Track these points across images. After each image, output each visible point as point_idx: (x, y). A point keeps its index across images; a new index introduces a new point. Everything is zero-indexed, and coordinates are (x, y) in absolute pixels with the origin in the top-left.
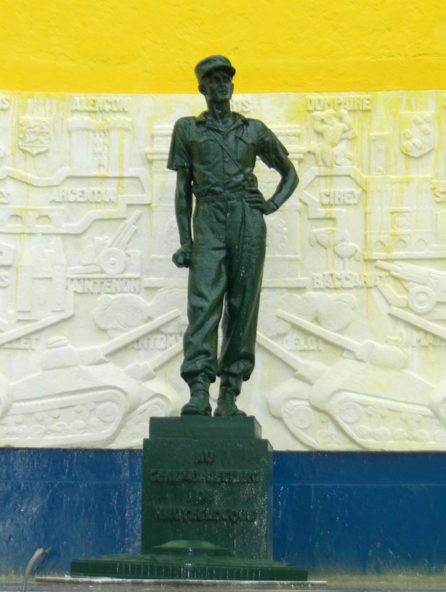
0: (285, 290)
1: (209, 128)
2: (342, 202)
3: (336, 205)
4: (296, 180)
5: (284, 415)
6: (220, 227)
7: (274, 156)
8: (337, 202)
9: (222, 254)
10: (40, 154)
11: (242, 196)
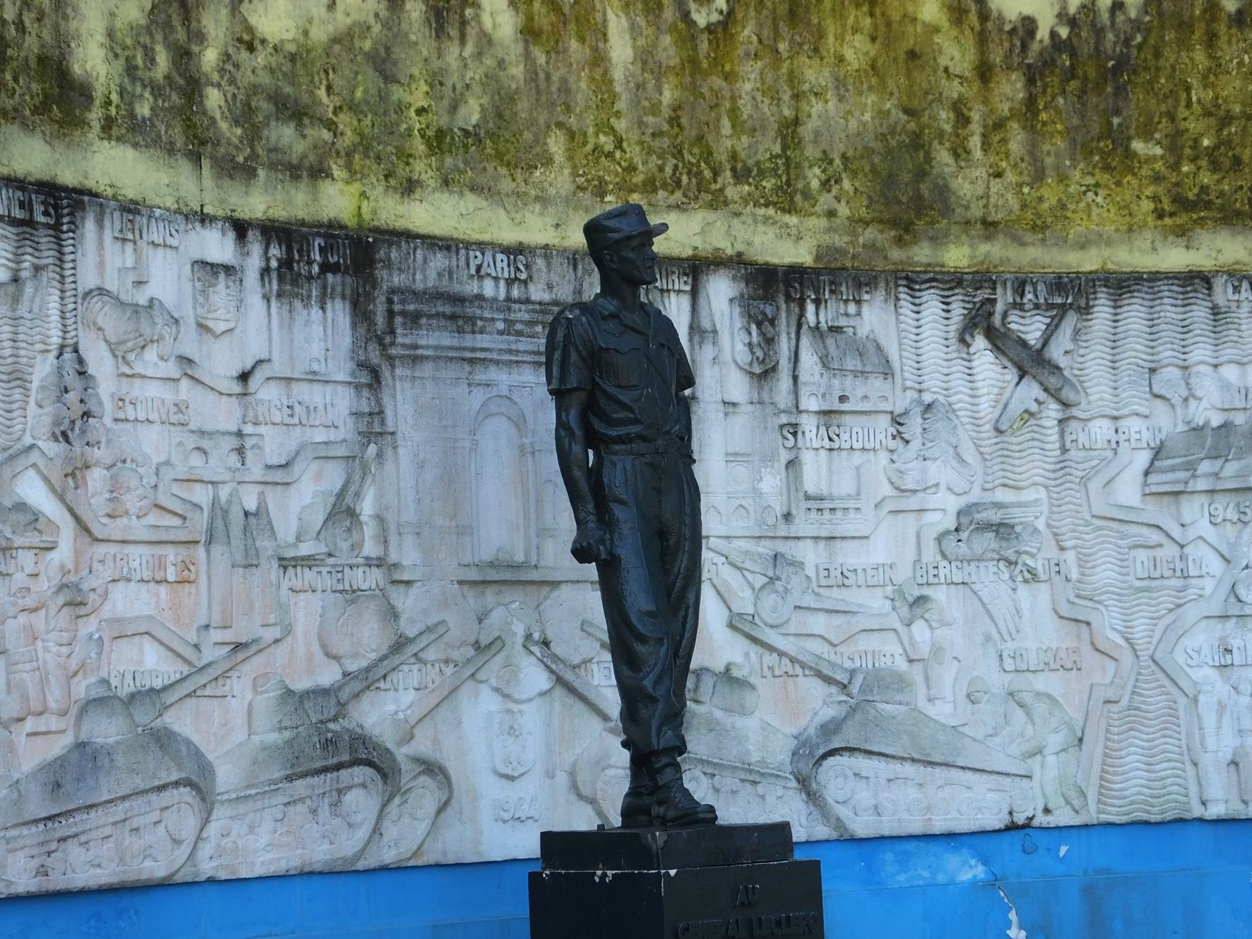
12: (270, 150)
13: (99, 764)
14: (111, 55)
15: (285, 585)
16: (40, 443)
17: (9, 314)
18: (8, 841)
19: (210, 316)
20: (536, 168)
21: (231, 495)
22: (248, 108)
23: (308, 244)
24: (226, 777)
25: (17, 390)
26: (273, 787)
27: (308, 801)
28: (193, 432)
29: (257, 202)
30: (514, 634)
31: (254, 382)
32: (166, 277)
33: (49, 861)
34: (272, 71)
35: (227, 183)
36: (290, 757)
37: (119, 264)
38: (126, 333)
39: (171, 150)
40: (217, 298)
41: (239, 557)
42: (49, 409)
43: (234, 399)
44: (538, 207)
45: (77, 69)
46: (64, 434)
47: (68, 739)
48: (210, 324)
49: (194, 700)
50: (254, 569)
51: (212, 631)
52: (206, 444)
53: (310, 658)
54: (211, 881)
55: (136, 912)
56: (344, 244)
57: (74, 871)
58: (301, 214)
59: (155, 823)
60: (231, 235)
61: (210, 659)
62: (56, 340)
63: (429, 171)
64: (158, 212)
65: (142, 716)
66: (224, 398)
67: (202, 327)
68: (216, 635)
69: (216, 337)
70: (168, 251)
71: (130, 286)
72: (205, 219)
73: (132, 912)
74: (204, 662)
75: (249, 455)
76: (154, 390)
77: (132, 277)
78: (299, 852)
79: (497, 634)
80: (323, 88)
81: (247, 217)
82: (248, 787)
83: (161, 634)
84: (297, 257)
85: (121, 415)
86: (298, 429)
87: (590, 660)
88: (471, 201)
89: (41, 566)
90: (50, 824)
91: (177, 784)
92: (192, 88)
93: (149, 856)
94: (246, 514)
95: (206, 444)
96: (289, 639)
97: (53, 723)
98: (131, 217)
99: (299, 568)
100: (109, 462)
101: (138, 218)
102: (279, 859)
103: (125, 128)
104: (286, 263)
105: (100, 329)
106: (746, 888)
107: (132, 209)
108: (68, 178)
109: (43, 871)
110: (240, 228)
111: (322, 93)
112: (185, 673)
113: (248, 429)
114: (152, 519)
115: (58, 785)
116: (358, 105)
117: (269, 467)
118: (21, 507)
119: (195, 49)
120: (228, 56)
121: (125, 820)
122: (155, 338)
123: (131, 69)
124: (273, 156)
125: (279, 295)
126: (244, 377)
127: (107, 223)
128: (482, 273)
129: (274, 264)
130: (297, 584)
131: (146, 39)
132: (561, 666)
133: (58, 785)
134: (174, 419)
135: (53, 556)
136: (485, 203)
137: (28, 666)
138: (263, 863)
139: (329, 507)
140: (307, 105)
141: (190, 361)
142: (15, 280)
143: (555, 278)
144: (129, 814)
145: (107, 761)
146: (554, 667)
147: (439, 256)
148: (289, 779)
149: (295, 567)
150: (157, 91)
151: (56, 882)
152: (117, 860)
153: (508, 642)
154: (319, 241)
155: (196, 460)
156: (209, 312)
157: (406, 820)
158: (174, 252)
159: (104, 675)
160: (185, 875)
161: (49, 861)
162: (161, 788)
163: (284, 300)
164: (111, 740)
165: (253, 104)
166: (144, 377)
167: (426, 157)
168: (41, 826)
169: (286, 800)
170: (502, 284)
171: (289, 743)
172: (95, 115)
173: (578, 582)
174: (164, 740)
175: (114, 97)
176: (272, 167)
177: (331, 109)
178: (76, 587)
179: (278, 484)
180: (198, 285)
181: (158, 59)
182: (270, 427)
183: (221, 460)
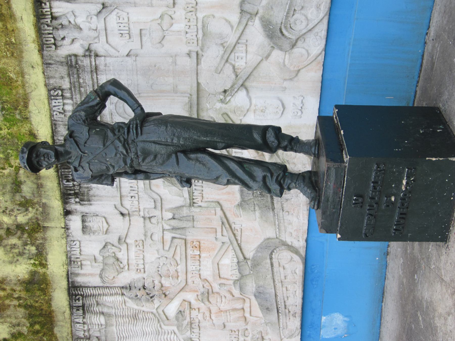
0: (199, 67)
1: (79, 165)
2: (127, 25)
3: (129, 28)
4: (115, 83)
5: (296, 69)
6: (159, 160)
7: (96, 108)
8: (127, 29)
9: (181, 156)
10: (107, 223)
11: (133, 141)
12: (34, 196)
13: (262, 292)
14: (18, 262)
15: (200, 204)
16: (156, 307)
17: (114, 317)
18: (284, 329)
19: (102, 230)
20: (9, 76)
21: (167, 224)
22: (20, 205)
23: (67, 187)
24: (270, 233)
25: (139, 316)
26: (276, 215)
27: (283, 202)
28: (145, 239)
29: (56, 204)
30: (221, 108)
31: (125, 212)
32: (90, 247)
33: (292, 313)
34: (4, 194)
35: (51, 216)
36: (265, 209)
37: (89, 267)
38: (114, 269)
39: (45, 239)
40: (95, 227)
41: (190, 224)
42: (144, 303)
43: (131, 218)
44: (26, 76)
45: (27, 276)
46: (151, 297)
47: (253, 298)
48: (105, 230)
49: (242, 243)
50: (195, 217)
51: (217, 237)
52: (149, 234)
53: (229, 193)
54: (307, 241)
55: (313, 265)
56: (64, 172)
57: (296, 302)
58: (56, 185)
59: (284, 269)
60: (70, 217)
61: (227, 238)
62: (120, 298)
63: (24, 126)
64: (69, 249)
65: (247, 272)
66: (131, 223)
67: (107, 232)
68: (219, 234)
69: (109, 226)
70: (82, 245)
71: (97, 264)
72: (66, 228)
73: (313, 267)
74: (228, 241)
75: (151, 215)
76: (132, 254)
77: (94, 263)
78: (301, 205)
79: (220, 116)
80: (4, 171)
81: (62, 209)
82: (275, 225)
83: (218, 258)
84: (73, 192)
85: (142, 270)
86: (140, 194)
87: (234, 67)
88: (31, 107)
89: (196, 307)
90: (280, 311)
91: (271, 259)
92: (19, 227)
93: (295, 271)
94: (174, 218)
95: (149, 234)
96: (221, 202)
97: (247, 305)
98: (73, 262)
99: (194, 197)
100: (159, 278)
101: (72, 259)
102: (303, 214)
103: (41, 257)
104: (76, 195)
105: (114, 277)
106: (354, 204)
107: (70, 261)
108: (64, 284)
109: (294, 315)
110: (67, 213)
111: (6, 172)
112: (232, 248)
113: (142, 214)
114: (178, 258)
115: (268, 309)
116: (6, 156)
117: (155, 208)
118: (177, 318)
119: (5, 226)
120: (4, 212)
121: (282, 282)
122: (113, 255)
123: (21, 254)
124: (36, 195)
125: (89, 201)
126: (122, 214)
127: (77, 272)
128: (62, 112)
129: (77, 200)
130: (200, 199)
131: (8, 247)
132: (236, 86)
133: (268, 309)
134: (141, 248)
135: (193, 302)
136: (31, 101)
137: (229, 317)
138: (304, 220)
139: (169, 184)
140: (12, 179)
141: (120, 239)
142: (103, 313)
143: (57, 75)
144: (280, 281)
145: (261, 288)
146: (236, 90)
147: (59, 129)
148: (273, 209)
149: (193, 199)
150: (25, 244)
151: (298, 310)
152: (295, 285)
153: (224, 111)
154: (65, 182)
155: (155, 237)
156: (101, 230)
157: (295, 161)
158: (82, 242)
159: (231, 282)
160: (303, 252)
161: (292, 313)
162: (272, 265)
163: (91, 199)
164: (254, 285)
165: (19, 203)
166: (128, 260)
167: (19, 127)
168: (280, 314)
169: (281, 211)
170: (66, 101)
171: (260, 208)
172: (41, 270)
173: (197, 73)
174: (256, 264)
175: (32, 261)
176: (40, 196)
177: (11, 169)
178: (203, 294)
179: (161, 204)
180: (91, 234)
181: (14, 243)
182: (140, 205)
183: (155, 229)
